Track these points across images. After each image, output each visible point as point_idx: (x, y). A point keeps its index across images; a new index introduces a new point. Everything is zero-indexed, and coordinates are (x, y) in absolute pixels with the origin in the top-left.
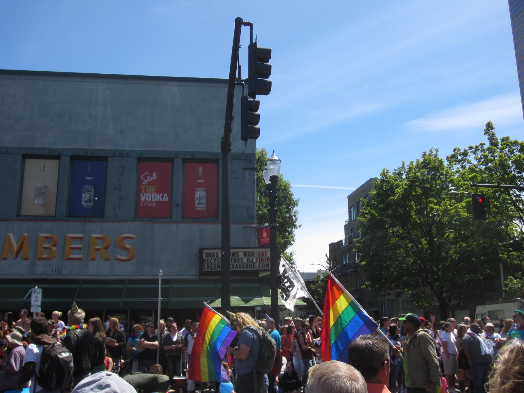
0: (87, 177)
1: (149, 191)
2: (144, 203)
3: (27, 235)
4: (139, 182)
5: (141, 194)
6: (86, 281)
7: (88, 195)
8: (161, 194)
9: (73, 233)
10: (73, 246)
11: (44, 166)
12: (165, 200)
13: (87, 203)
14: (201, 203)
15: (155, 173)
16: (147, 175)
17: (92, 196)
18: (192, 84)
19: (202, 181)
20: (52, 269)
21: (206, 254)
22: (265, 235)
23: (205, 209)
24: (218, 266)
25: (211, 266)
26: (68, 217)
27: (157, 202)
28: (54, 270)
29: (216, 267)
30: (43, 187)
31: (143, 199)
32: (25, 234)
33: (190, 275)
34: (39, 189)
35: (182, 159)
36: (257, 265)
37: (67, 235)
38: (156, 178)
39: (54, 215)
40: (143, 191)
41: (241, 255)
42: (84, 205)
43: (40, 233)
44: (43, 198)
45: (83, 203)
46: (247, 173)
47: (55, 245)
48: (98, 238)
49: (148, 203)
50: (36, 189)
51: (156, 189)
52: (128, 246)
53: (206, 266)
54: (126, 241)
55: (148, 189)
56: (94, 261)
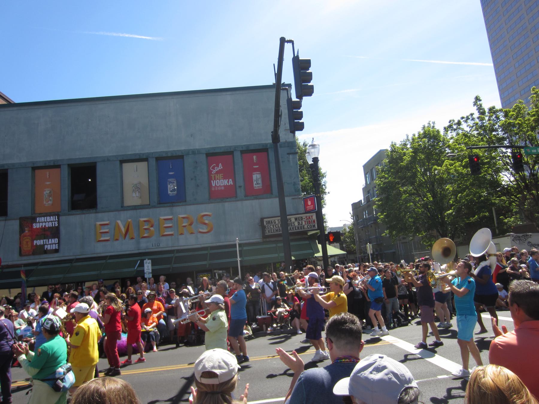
0: (170, 172)
1: (218, 178)
4: (209, 172)
5: (212, 181)
6: (178, 251)
7: (172, 186)
8: (227, 180)
9: (165, 215)
12: (231, 184)
14: (258, 184)
16: (214, 167)
18: (241, 92)
19: (257, 167)
20: (153, 244)
21: (266, 222)
22: (309, 203)
23: (261, 188)
24: (277, 230)
25: (271, 231)
26: (159, 204)
27: (224, 186)
28: (154, 245)
29: (275, 231)
31: (214, 185)
32: (130, 220)
36: (306, 226)
37: (160, 217)
38: (222, 168)
39: (149, 204)
41: (293, 220)
42: (170, 194)
43: (140, 218)
44: (139, 192)
45: (169, 192)
46: (291, 156)
47: (152, 226)
48: (183, 218)
50: (133, 185)
51: (222, 177)
52: (207, 222)
53: (267, 231)
54: (205, 218)
55: (216, 177)
56: (183, 235)
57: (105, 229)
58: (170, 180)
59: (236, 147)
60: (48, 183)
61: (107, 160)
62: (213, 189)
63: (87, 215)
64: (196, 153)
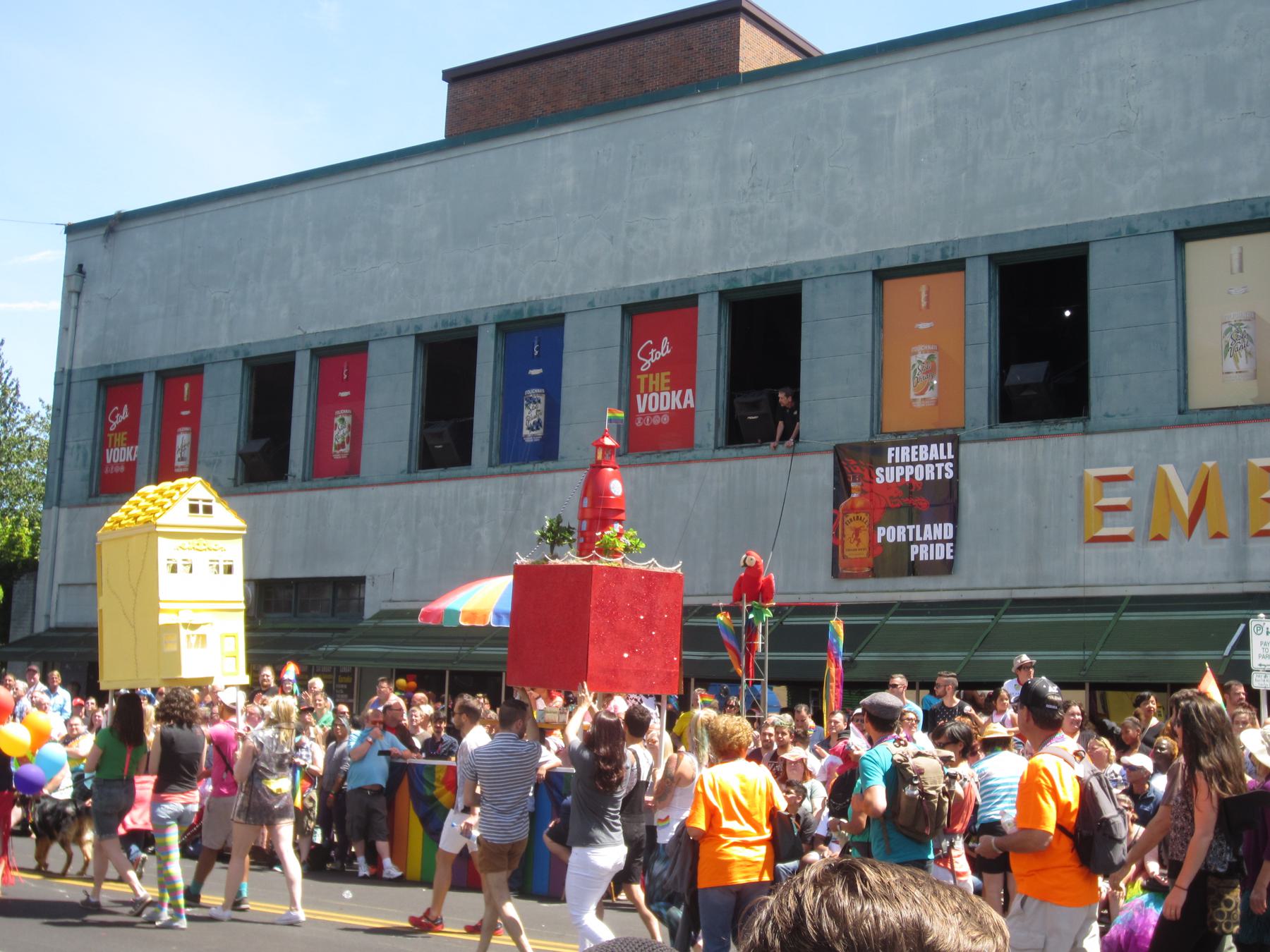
0: (532, 369)
1: (654, 386)
2: (644, 417)
3: (1214, 465)
4: (634, 365)
5: (639, 397)
7: (534, 413)
8: (680, 392)
10: (1104, 502)
11: (1241, 255)
12: (689, 405)
13: (533, 430)
14: (182, 459)
15: (666, 339)
16: (648, 348)
17: (541, 414)
30: (1245, 320)
31: (641, 410)
32: (1210, 464)
33: (708, 595)
34: (1235, 326)
35: (1172, 234)
38: (668, 351)
40: (642, 389)
42: (526, 436)
43: (1253, 456)
44: (1249, 354)
45: (526, 432)
49: (652, 416)
50: (1227, 326)
51: (668, 381)
55: (651, 383)
57: (1116, 495)
58: (530, 392)
59: (968, 240)
60: (344, 394)
61: (1129, 231)
62: (639, 423)
63: (1052, 442)
64: (1124, 234)
